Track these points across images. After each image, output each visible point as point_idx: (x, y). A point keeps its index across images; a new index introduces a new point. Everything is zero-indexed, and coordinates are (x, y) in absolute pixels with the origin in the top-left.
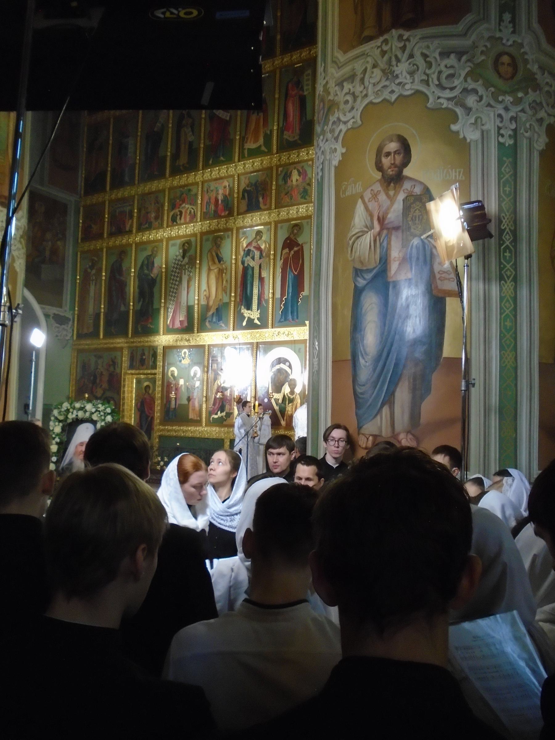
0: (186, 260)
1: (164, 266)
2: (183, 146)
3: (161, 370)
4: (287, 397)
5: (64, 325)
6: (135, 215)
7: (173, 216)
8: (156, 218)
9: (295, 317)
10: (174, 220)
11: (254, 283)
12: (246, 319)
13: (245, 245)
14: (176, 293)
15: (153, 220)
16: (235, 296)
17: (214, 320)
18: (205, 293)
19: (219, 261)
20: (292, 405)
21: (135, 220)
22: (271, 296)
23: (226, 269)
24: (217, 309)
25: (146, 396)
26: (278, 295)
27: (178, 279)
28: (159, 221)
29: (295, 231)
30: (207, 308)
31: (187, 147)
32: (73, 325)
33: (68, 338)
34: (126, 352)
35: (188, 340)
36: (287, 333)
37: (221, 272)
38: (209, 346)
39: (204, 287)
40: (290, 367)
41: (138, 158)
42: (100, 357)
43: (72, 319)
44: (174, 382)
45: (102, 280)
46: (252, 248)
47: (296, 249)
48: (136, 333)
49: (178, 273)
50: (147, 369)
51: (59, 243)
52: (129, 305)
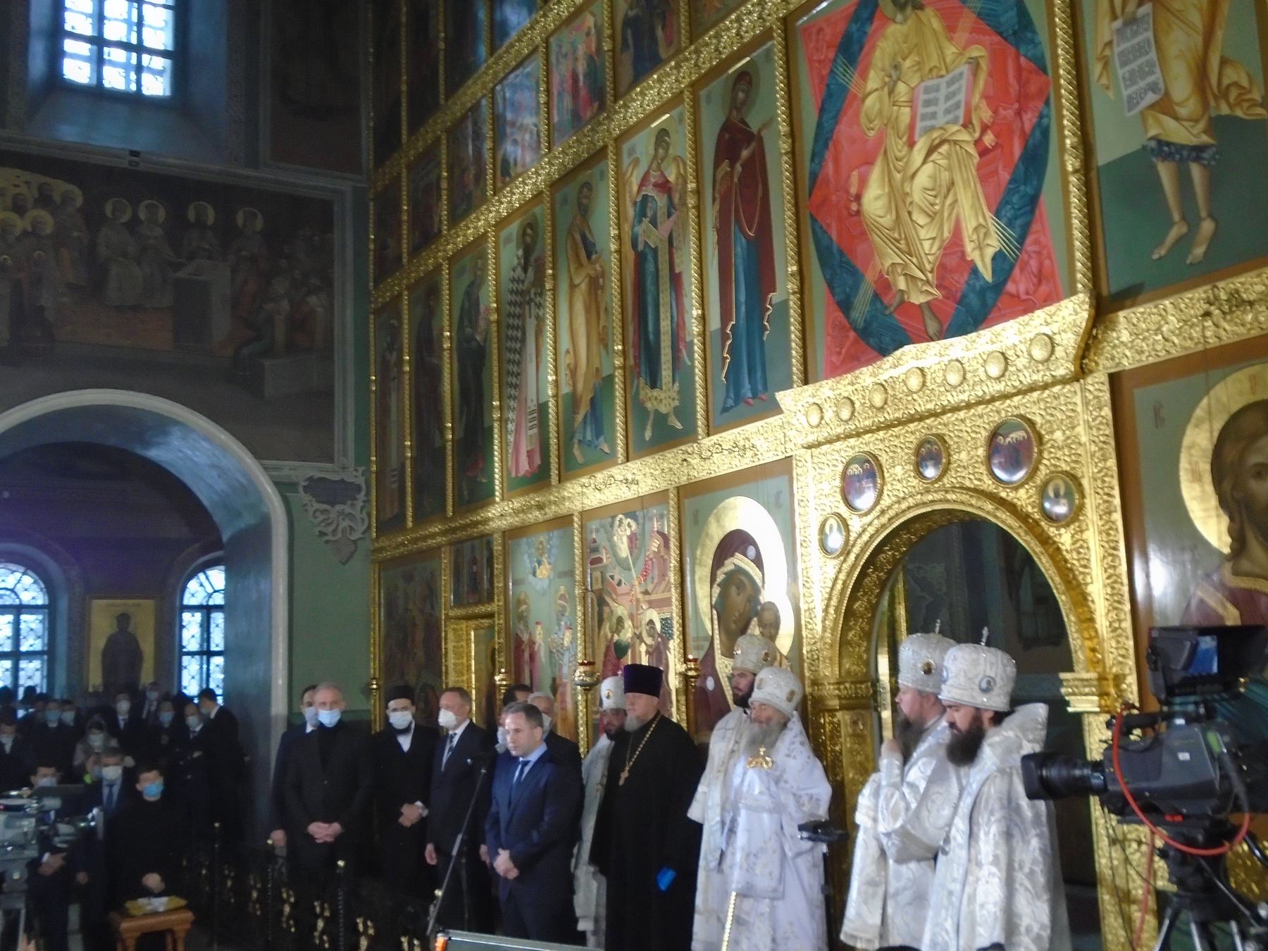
3: (501, 603)
5: (344, 503)
6: (444, 185)
9: (760, 387)
10: (506, 172)
11: (661, 295)
12: (651, 418)
13: (635, 188)
15: (472, 187)
17: (589, 437)
18: (568, 362)
19: (589, 257)
23: (603, 274)
27: (519, 335)
29: (741, 95)
32: (367, 501)
33: (354, 537)
34: (446, 561)
35: (540, 507)
38: (582, 513)
39: (565, 343)
40: (758, 562)
41: (443, 35)
42: (409, 578)
43: (364, 486)
44: (525, 638)
45: (404, 373)
46: (650, 191)
47: (745, 153)
51: (313, 300)
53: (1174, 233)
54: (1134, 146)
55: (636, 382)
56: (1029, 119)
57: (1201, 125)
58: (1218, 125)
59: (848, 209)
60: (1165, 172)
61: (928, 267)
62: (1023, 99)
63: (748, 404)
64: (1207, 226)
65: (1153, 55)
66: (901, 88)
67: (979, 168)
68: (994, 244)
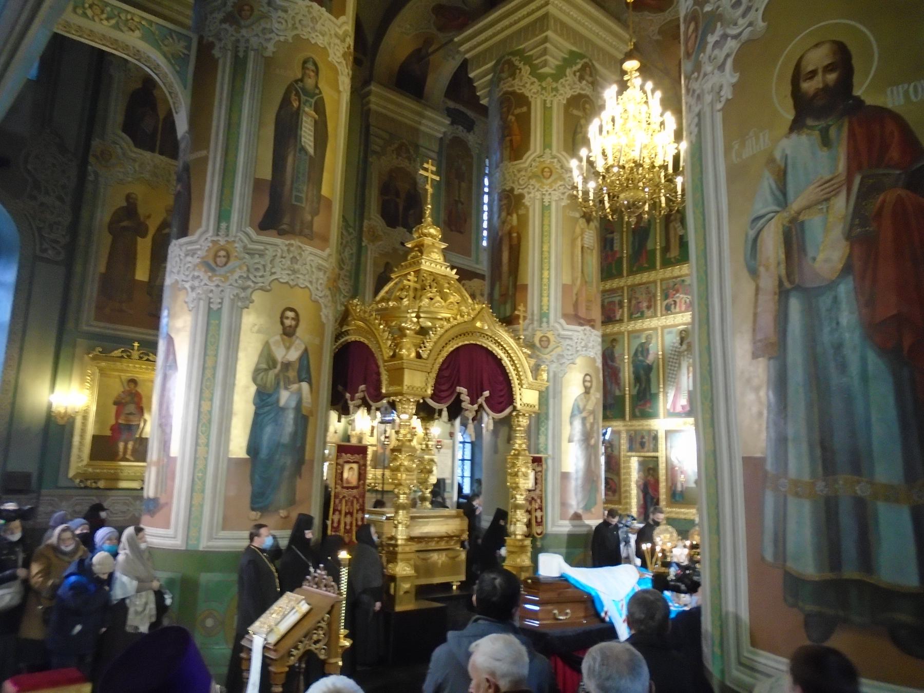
0: (684, 347)
1: (660, 353)
2: (672, 240)
6: (626, 305)
7: (667, 305)
8: (649, 307)
14: (675, 378)
21: (626, 310)
25: (650, 478)
28: (652, 310)
31: (677, 237)
34: (624, 435)
48: (634, 417)
50: (648, 451)
52: (625, 390)
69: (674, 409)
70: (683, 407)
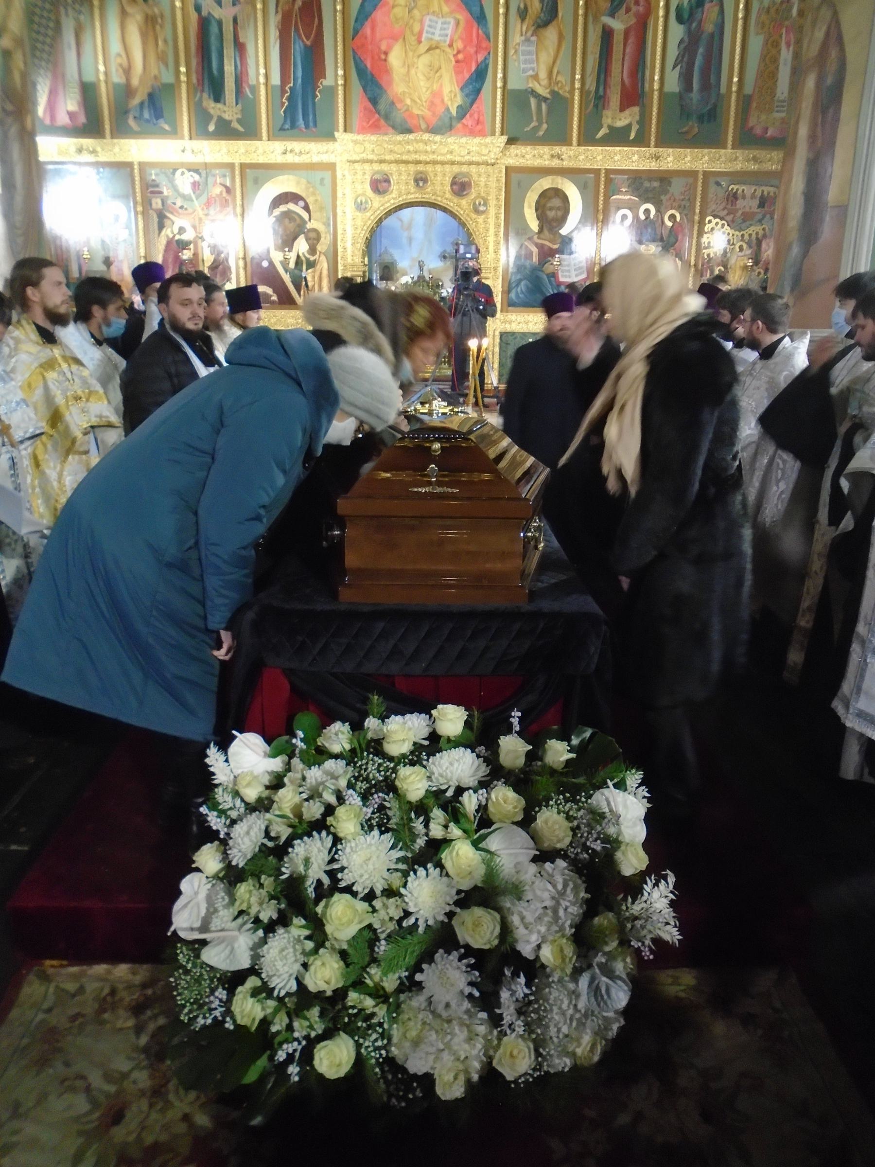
4: (303, 259)
9: (311, 124)
11: (225, 51)
12: (215, 119)
14: (50, 54)
16: (188, 74)
17: (146, 115)
18: (119, 60)
20: (314, 272)
22: (262, 80)
23: (162, 16)
24: (151, 96)
26: (276, 79)
30: (127, 91)
35: (94, 152)
36: (297, 151)
37: (151, 23)
40: (307, 208)
49: (50, 11)
53: (533, 124)
54: (522, 86)
55: (198, 95)
56: (480, 58)
57: (548, 90)
58: (553, 93)
59: (379, 57)
60: (533, 102)
61: (424, 100)
62: (478, 49)
63: (301, 130)
64: (545, 126)
65: (534, 57)
66: (416, 12)
67: (455, 67)
68: (459, 101)
69: (53, 117)
70: (71, 115)
